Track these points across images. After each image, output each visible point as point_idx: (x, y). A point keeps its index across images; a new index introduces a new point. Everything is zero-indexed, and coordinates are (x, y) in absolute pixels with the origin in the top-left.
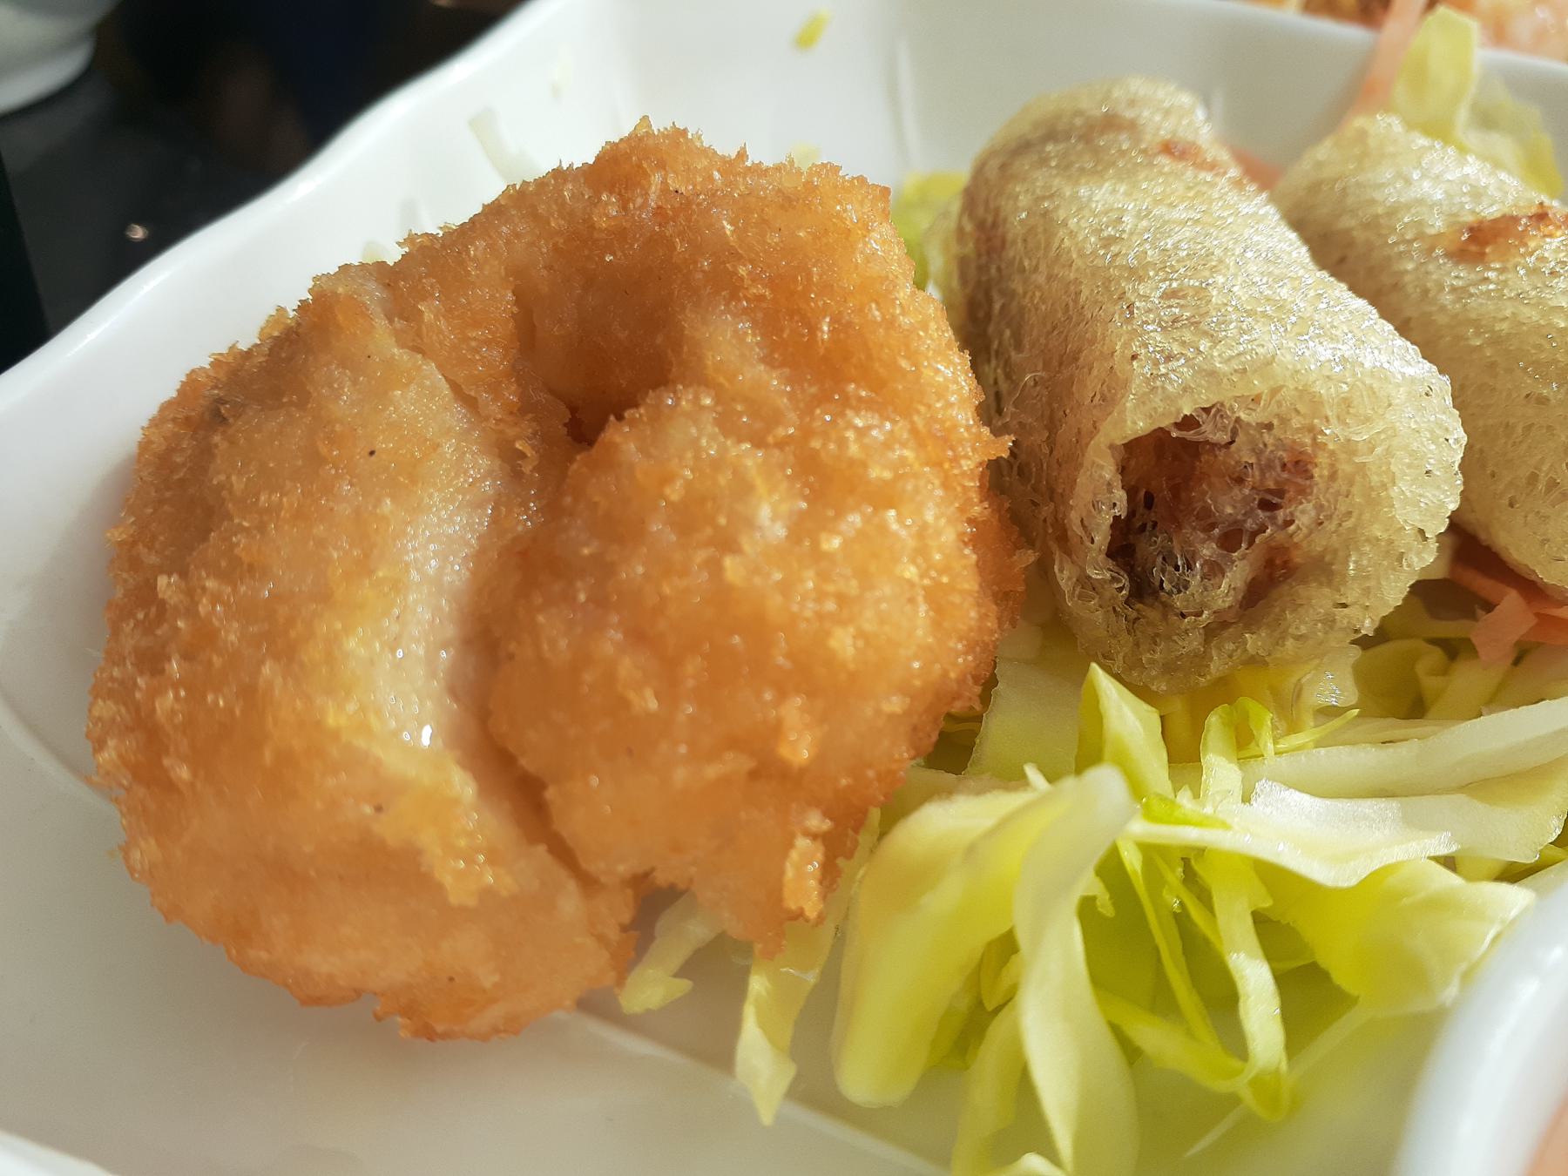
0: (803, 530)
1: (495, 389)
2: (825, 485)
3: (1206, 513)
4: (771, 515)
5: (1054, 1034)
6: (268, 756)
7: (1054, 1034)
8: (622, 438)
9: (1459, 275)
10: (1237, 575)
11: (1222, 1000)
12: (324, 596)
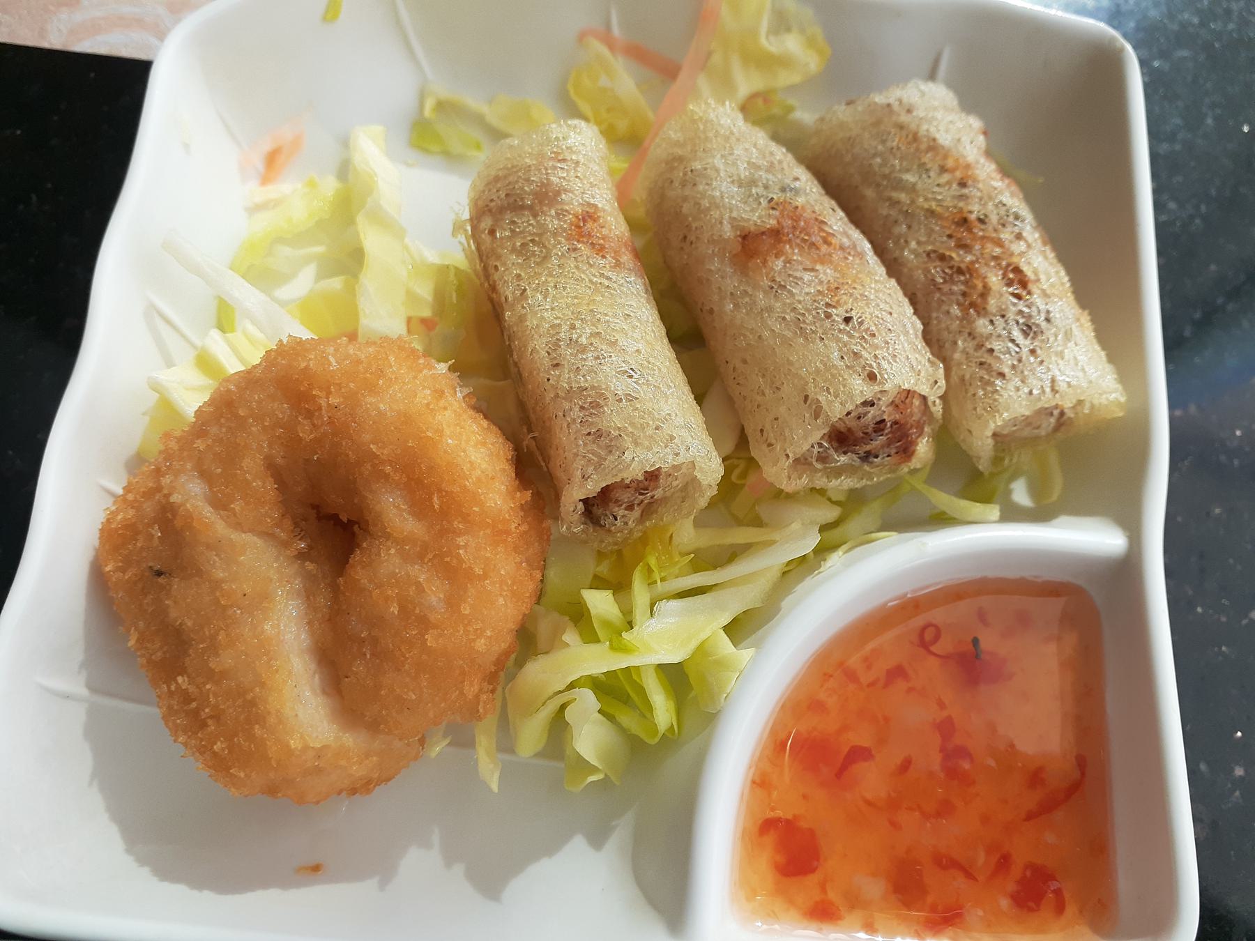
0: (452, 603)
1: (277, 525)
2: (455, 575)
3: (617, 501)
4: (435, 595)
5: (590, 738)
6: (274, 763)
7: (590, 738)
8: (359, 573)
9: (731, 282)
10: (637, 513)
11: (650, 708)
12: (262, 685)
